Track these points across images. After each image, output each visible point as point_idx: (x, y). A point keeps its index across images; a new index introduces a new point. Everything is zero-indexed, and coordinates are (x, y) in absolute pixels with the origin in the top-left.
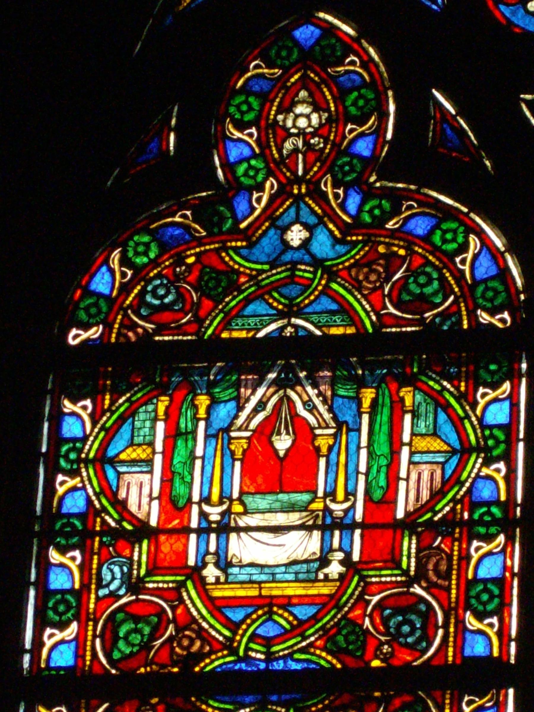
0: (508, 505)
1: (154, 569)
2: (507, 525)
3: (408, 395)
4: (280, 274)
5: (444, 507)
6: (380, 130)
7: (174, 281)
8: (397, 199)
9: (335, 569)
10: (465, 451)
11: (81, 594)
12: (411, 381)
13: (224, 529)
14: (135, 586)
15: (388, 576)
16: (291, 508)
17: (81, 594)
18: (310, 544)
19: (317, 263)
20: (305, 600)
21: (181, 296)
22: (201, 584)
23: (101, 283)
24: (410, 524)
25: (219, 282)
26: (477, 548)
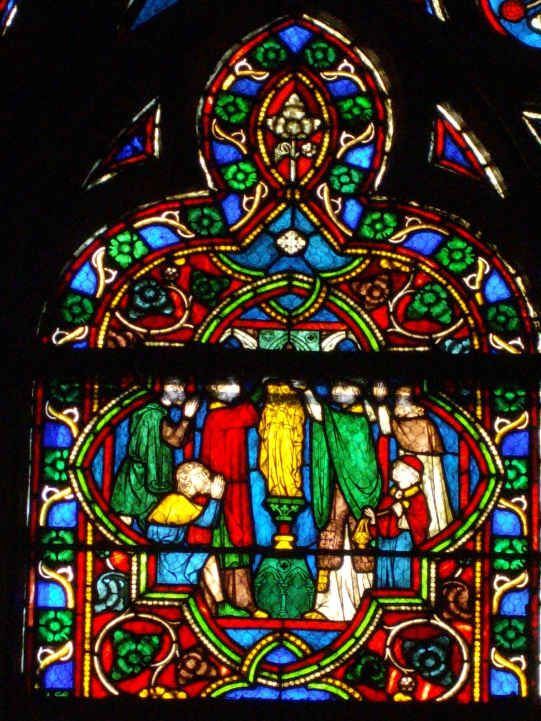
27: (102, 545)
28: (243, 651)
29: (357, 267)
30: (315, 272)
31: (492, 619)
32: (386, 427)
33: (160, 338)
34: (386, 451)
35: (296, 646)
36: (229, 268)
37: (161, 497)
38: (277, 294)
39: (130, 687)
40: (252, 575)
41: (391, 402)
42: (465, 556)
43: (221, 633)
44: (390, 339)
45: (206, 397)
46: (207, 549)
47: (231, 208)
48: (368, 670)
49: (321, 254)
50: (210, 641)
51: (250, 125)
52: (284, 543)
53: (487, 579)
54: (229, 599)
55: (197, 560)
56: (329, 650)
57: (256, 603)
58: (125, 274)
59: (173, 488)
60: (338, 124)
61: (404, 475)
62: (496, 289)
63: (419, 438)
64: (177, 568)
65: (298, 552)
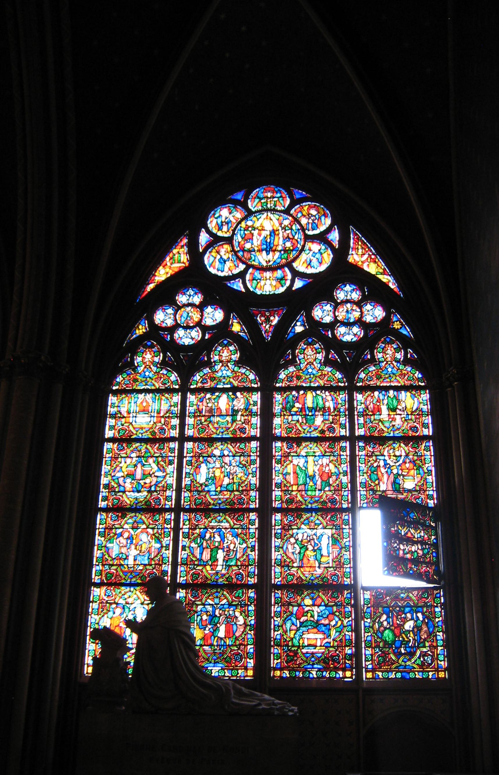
0: (177, 414)
1: (126, 423)
2: (177, 417)
3: (163, 398)
4: (144, 379)
5: (168, 415)
6: (159, 359)
7: (129, 380)
8: (162, 369)
9: (152, 423)
10: (171, 406)
11: (114, 426)
12: (163, 396)
13: (136, 417)
14: (123, 425)
15: (160, 424)
16: (145, 414)
17: (114, 426)
18: (149, 419)
19: (150, 378)
20: (148, 428)
21: (130, 382)
22: (132, 425)
23: (118, 380)
24: (163, 417)
25: (135, 380)
26: (172, 420)
27: (284, 415)
28: (305, 430)
29: (320, 374)
30: (314, 375)
31: (341, 424)
32: (324, 397)
33: (293, 384)
34: (324, 400)
35: (312, 429)
36: (301, 375)
37: (293, 408)
38: (308, 378)
39: (289, 435)
40: (306, 419)
41: (325, 393)
42: (336, 415)
43: (302, 427)
44: (325, 384)
45: (298, 393)
46: (299, 415)
47: (301, 365)
48: (323, 432)
49: (314, 372)
50: (300, 428)
51: (304, 353)
52: (310, 414)
53: (339, 418)
54: (303, 422)
55: (298, 416)
56: (317, 429)
57: (306, 423)
58: (287, 376)
59: (294, 406)
60: (316, 353)
61: (327, 404)
62: (340, 376)
63: (329, 398)
64: (295, 418)
65: (312, 415)
